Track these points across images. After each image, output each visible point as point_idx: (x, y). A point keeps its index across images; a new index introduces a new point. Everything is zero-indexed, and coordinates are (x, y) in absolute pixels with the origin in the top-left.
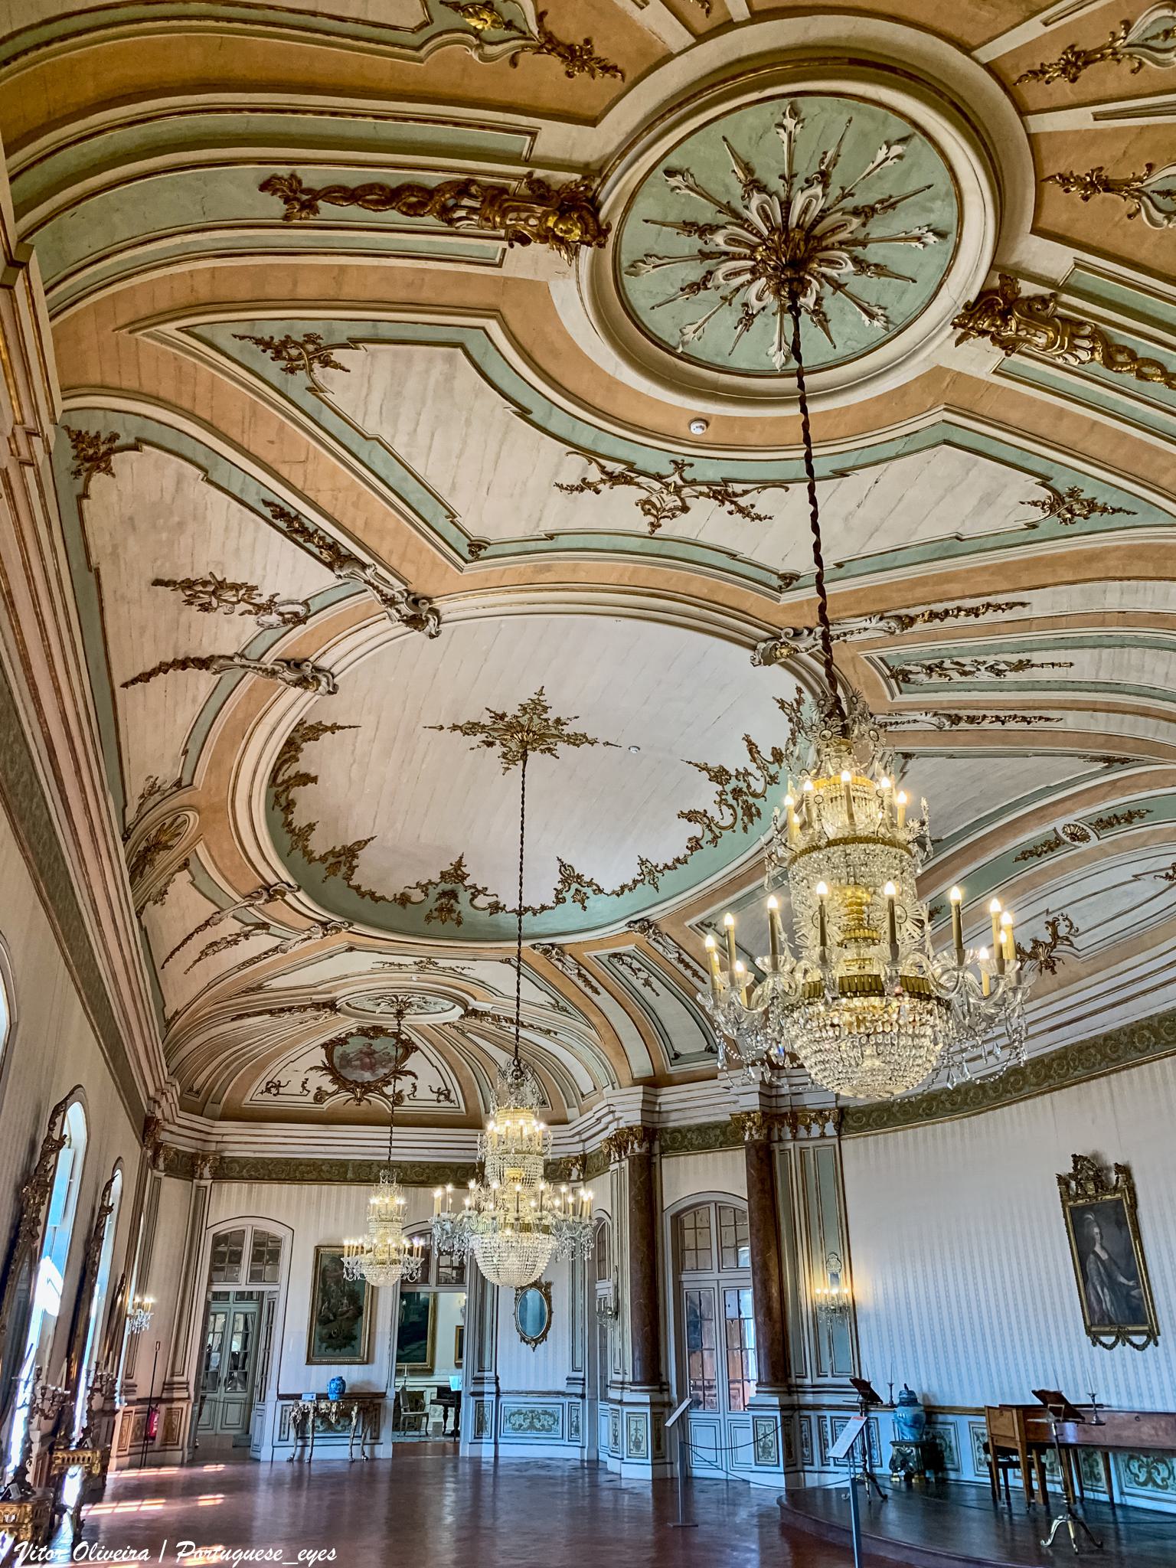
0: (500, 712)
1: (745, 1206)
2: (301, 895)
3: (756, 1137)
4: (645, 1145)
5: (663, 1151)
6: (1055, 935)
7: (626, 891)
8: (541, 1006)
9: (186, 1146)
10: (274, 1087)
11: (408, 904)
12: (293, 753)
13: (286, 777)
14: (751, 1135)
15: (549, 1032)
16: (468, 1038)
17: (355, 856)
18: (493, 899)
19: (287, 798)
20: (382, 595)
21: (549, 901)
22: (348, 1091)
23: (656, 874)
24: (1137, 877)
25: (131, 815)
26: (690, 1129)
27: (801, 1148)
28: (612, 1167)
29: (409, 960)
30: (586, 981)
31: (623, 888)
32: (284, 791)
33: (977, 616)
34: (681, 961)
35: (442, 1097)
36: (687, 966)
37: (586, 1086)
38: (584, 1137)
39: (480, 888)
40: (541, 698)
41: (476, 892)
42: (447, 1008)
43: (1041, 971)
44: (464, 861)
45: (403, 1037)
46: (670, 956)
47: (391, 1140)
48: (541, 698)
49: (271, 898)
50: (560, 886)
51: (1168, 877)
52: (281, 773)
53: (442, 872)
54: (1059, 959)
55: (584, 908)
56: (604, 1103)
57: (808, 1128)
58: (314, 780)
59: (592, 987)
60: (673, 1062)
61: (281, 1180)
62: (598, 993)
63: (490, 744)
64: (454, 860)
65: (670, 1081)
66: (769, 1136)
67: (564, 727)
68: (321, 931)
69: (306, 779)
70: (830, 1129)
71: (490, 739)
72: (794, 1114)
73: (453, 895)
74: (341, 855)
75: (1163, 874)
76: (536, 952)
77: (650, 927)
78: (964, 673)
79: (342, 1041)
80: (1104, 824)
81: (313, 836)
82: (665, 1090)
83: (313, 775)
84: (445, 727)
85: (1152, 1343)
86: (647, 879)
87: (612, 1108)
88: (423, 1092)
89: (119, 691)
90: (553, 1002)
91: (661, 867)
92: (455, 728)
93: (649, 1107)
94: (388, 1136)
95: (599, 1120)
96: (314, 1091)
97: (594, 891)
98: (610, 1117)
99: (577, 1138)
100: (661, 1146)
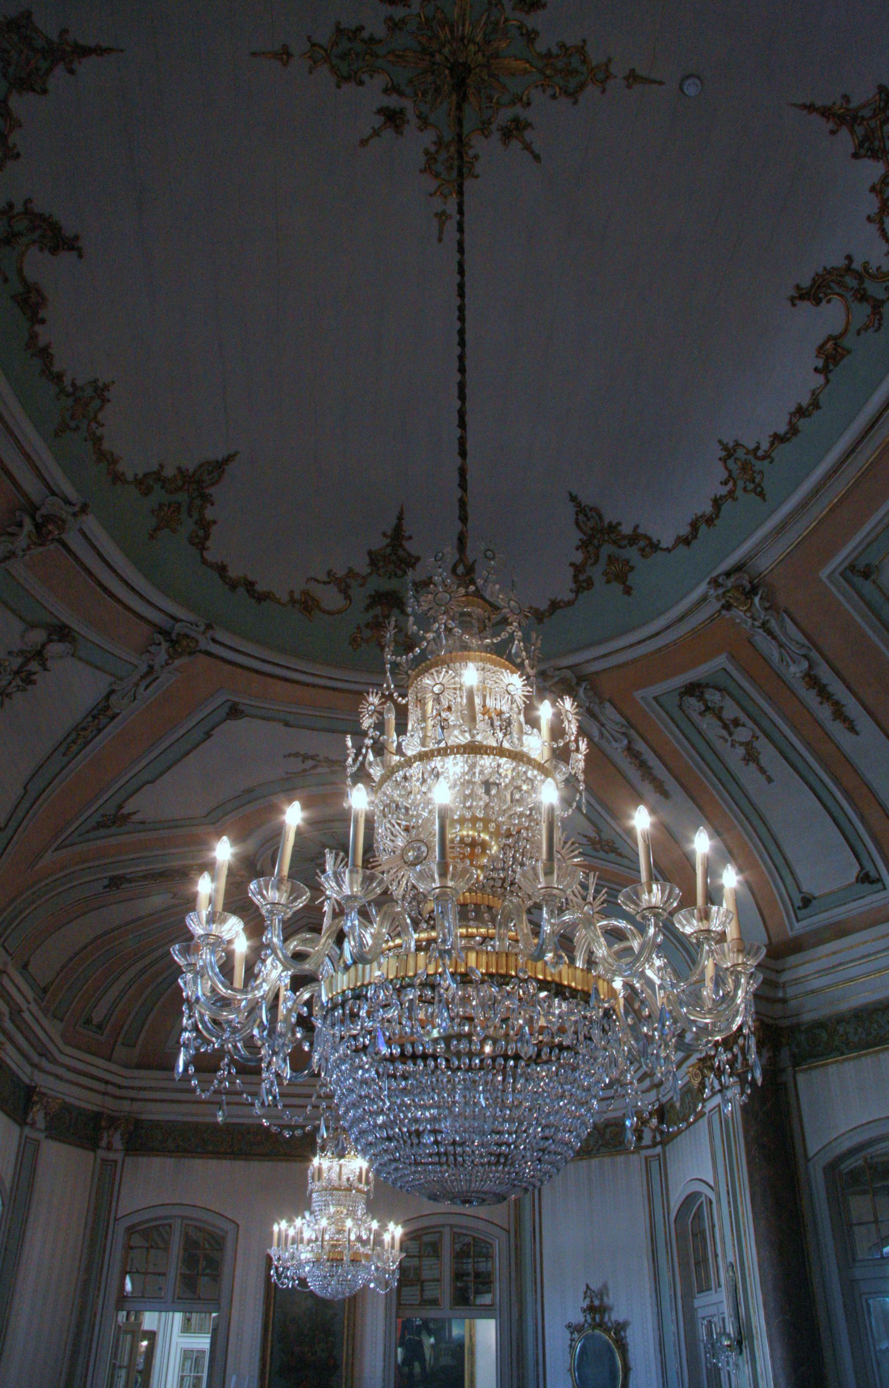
5: (797, 1060)
7: (703, 528)
21: (564, 590)
23: (758, 465)
26: (840, 1019)
31: (694, 526)
34: (812, 680)
36: (824, 693)
46: (793, 669)
55: (628, 591)
60: (801, 913)
61: (218, 1155)
65: (796, 946)
71: (393, 101)
77: (754, 590)
82: (792, 960)
86: (741, 484)
91: (765, 445)
97: (642, 550)
100: (793, 1056)
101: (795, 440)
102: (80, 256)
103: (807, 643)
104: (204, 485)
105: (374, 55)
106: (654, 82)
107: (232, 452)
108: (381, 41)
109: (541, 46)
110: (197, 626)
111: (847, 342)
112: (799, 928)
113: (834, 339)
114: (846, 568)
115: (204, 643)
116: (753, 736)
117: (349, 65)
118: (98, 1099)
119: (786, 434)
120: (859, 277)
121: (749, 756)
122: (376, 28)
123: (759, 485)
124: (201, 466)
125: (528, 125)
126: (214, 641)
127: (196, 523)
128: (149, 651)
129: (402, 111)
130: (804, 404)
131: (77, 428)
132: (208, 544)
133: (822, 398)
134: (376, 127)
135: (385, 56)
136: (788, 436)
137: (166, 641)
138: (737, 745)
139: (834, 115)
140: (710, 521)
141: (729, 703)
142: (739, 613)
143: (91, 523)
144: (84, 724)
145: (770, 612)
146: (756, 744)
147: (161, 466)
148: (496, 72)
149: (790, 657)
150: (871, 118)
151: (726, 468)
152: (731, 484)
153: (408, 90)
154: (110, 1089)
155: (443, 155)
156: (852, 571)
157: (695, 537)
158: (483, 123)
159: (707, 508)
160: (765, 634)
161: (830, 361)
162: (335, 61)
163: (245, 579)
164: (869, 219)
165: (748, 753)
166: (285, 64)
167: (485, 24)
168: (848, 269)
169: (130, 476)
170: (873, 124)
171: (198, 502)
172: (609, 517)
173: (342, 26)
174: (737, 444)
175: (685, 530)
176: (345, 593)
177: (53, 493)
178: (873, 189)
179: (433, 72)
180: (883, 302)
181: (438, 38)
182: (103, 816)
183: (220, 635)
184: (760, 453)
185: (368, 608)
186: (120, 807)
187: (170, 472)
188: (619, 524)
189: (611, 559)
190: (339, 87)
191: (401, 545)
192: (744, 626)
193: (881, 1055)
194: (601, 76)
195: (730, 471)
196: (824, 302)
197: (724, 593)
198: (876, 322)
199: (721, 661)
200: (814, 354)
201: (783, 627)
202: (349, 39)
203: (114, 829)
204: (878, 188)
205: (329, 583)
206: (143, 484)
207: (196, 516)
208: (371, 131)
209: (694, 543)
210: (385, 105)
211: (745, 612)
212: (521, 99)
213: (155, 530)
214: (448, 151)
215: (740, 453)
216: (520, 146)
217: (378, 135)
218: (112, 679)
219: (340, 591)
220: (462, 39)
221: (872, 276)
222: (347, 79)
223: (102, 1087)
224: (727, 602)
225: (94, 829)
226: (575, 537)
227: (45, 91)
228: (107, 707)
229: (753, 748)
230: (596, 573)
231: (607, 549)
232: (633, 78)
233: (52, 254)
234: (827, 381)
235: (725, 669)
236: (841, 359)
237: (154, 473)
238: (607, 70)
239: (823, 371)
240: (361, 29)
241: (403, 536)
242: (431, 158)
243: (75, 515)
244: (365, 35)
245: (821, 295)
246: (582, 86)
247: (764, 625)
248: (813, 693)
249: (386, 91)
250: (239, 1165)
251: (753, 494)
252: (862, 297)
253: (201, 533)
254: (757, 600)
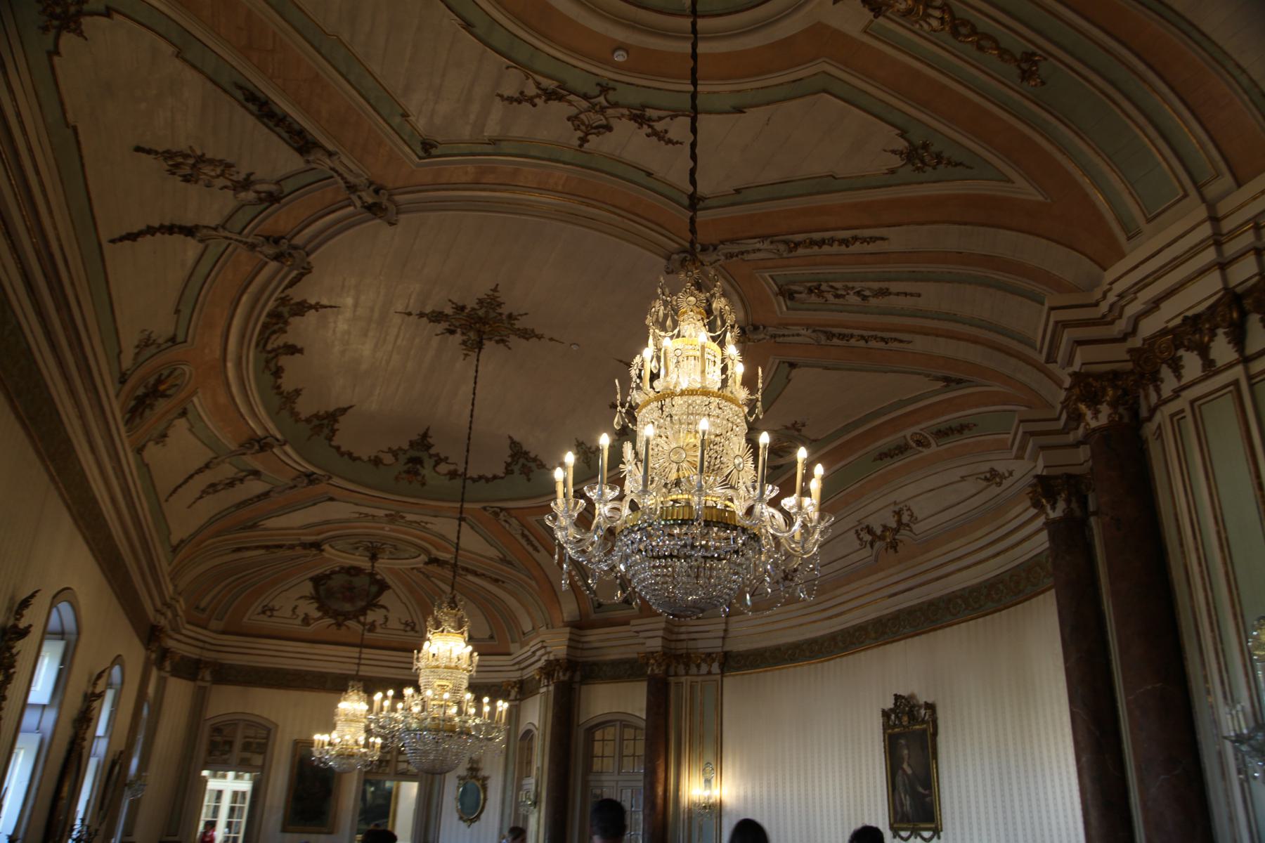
0: (460, 304)
1: (643, 724)
2: (288, 448)
3: (656, 671)
4: (568, 674)
6: (899, 522)
8: (491, 559)
9: (191, 652)
10: (268, 610)
12: (281, 325)
13: (275, 346)
14: (652, 670)
15: (496, 581)
16: (432, 582)
17: (336, 421)
18: (452, 467)
19: (276, 364)
20: (346, 182)
21: (500, 471)
22: (331, 617)
24: (963, 478)
25: (127, 362)
27: (692, 682)
28: (543, 690)
29: (382, 513)
30: (528, 540)
32: (274, 358)
33: (847, 246)
35: (408, 628)
37: (527, 626)
38: (523, 665)
39: (442, 456)
40: (496, 294)
41: (439, 460)
42: (414, 555)
43: (886, 549)
44: (430, 433)
45: (378, 577)
47: (360, 658)
48: (496, 294)
49: (262, 449)
50: (509, 460)
51: (986, 479)
52: (271, 341)
53: (411, 442)
54: (901, 541)
55: (529, 480)
56: (539, 639)
57: (698, 666)
58: (300, 351)
59: (533, 545)
62: (538, 551)
63: (452, 332)
64: (422, 432)
66: (667, 672)
67: (516, 322)
68: (306, 481)
69: (292, 350)
70: (715, 668)
71: (452, 328)
72: (688, 655)
73: (417, 461)
74: (324, 419)
75: (983, 476)
76: (487, 513)
78: (837, 296)
79: (327, 577)
80: (942, 434)
81: (300, 400)
82: (589, 632)
83: (299, 347)
84: (414, 312)
85: (935, 838)
87: (545, 644)
88: (394, 623)
89: (107, 247)
90: (501, 556)
92: (421, 315)
93: (573, 644)
94: (357, 655)
95: (534, 653)
96: (302, 616)
97: (538, 465)
98: (542, 651)
99: (517, 667)
112: (593, 616)
118: (198, 651)
132: (334, 438)
143: (288, 448)
154: (207, 646)
172: (525, 448)
189: (523, 465)
222: (434, 322)
223: (201, 644)
226: (509, 452)
230: (516, 468)
231: (522, 461)
250: (282, 692)
253: (331, 434)
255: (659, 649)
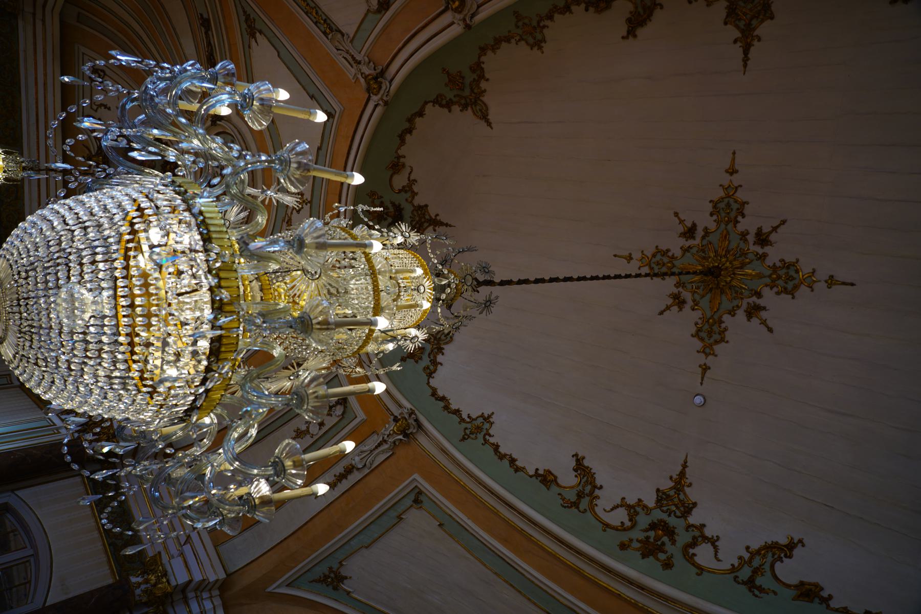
3: (138, 592)
7: (442, 404)
11: (391, 172)
14: (139, 584)
23: (480, 436)
31: (443, 399)
58: (631, 33)
64: (443, 218)
71: (700, 233)
77: (406, 436)
86: (469, 426)
91: (492, 440)
97: (428, 368)
101: (496, 457)
102: (623, 38)
103: (373, 467)
104: (473, 106)
105: (727, 223)
106: (702, 379)
107: (493, 125)
108: (735, 227)
109: (726, 318)
110: (387, 96)
111: (554, 488)
113: (555, 480)
114: (419, 488)
115: (375, 98)
116: (313, 435)
117: (723, 209)
119: (500, 453)
120: (591, 494)
121: (300, 433)
122: (743, 224)
123: (469, 437)
124: (485, 104)
125: (681, 309)
126: (376, 106)
127: (450, 99)
128: (370, 62)
129: (693, 238)
130: (517, 463)
131: (517, 27)
132: (437, 106)
133: (520, 474)
134: (685, 223)
135: (726, 229)
136: (498, 454)
137: (377, 74)
138: (307, 425)
139: (681, 479)
140: (447, 408)
141: (335, 420)
142: (391, 427)
144: (320, 13)
145: (392, 445)
146: (308, 436)
147: (487, 80)
148: (713, 292)
149: (365, 457)
150: (679, 499)
151: (478, 417)
152: (468, 420)
153: (705, 242)
155: (666, 260)
156: (418, 492)
157: (436, 399)
158: (684, 283)
159: (454, 406)
160: (379, 442)
161: (543, 478)
162: (726, 200)
163: (413, 129)
164: (623, 499)
165: (302, 432)
166: (727, 171)
167: (741, 287)
168: (595, 487)
169: (483, 59)
170: (676, 500)
171: (463, 101)
172: (448, 349)
173: (746, 205)
174: (492, 424)
175: (440, 393)
176: (402, 190)
177: (479, 7)
178: (640, 500)
179: (715, 256)
180: (578, 508)
181: (735, 260)
182: (254, 20)
183: (379, 110)
184: (487, 437)
185: (393, 204)
186: (261, 32)
187: (483, 85)
188: (443, 354)
190: (711, 201)
191: (430, 225)
192: (384, 429)
193: (96, 532)
194: (707, 350)
195: (476, 419)
196: (576, 474)
197: (405, 418)
198: (567, 505)
199: (361, 415)
200: (546, 468)
201: (383, 452)
202: (738, 209)
203: (244, 26)
204: (641, 504)
205: (409, 180)
206: (478, 69)
207: (455, 100)
208: (683, 219)
209: (433, 399)
210: (697, 228)
211: (393, 430)
212: (696, 305)
213: (448, 73)
214: (668, 263)
215: (487, 426)
216: (669, 304)
217: (680, 223)
218: (351, 36)
219: (404, 187)
220: (734, 274)
221: (591, 502)
222: (715, 207)
224: (399, 419)
225: (245, 12)
227: (726, 23)
228: (332, 30)
229: (306, 434)
232: (705, 369)
233: (628, 19)
234: (531, 476)
235: (356, 417)
236: (544, 484)
237: (484, 75)
238: (710, 354)
239: (537, 474)
240: (743, 216)
241: (436, 226)
242: (665, 253)
243: (464, 20)
244: (740, 218)
245: (579, 472)
246: (702, 340)
247: (384, 441)
248: (342, 471)
249: (706, 229)
251: (463, 434)
252: (580, 495)
254: (401, 437)
255: (173, 583)
